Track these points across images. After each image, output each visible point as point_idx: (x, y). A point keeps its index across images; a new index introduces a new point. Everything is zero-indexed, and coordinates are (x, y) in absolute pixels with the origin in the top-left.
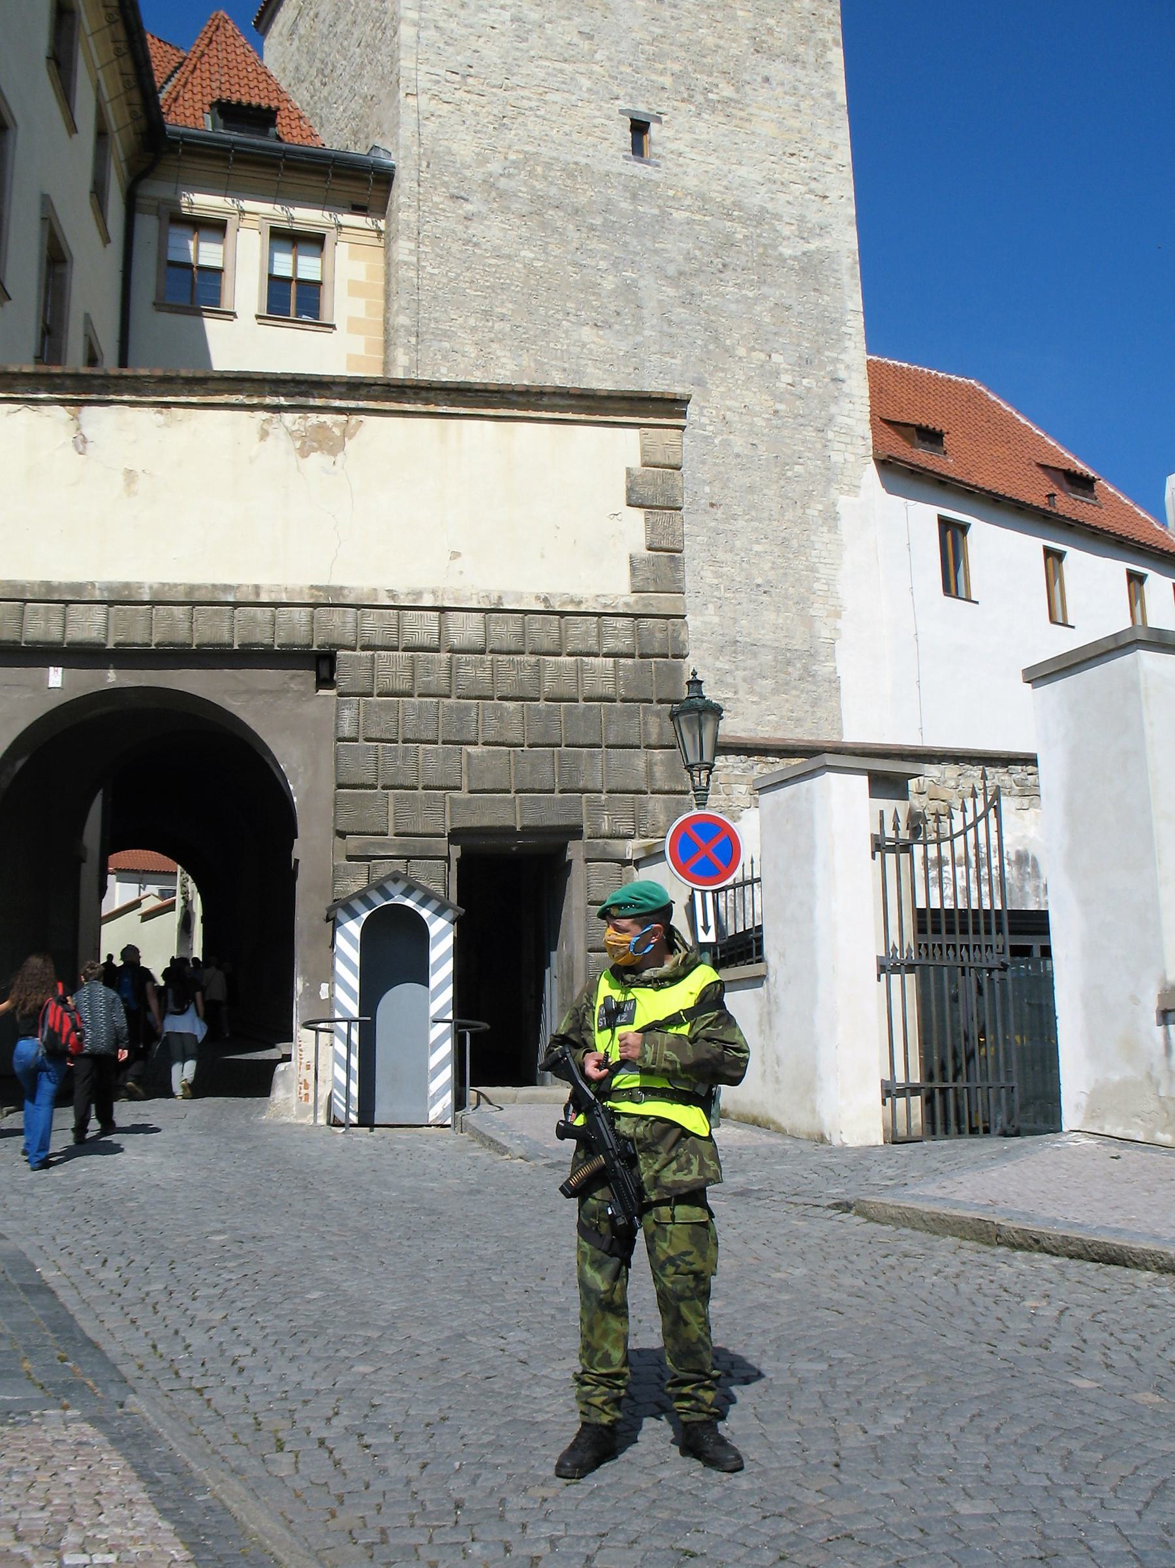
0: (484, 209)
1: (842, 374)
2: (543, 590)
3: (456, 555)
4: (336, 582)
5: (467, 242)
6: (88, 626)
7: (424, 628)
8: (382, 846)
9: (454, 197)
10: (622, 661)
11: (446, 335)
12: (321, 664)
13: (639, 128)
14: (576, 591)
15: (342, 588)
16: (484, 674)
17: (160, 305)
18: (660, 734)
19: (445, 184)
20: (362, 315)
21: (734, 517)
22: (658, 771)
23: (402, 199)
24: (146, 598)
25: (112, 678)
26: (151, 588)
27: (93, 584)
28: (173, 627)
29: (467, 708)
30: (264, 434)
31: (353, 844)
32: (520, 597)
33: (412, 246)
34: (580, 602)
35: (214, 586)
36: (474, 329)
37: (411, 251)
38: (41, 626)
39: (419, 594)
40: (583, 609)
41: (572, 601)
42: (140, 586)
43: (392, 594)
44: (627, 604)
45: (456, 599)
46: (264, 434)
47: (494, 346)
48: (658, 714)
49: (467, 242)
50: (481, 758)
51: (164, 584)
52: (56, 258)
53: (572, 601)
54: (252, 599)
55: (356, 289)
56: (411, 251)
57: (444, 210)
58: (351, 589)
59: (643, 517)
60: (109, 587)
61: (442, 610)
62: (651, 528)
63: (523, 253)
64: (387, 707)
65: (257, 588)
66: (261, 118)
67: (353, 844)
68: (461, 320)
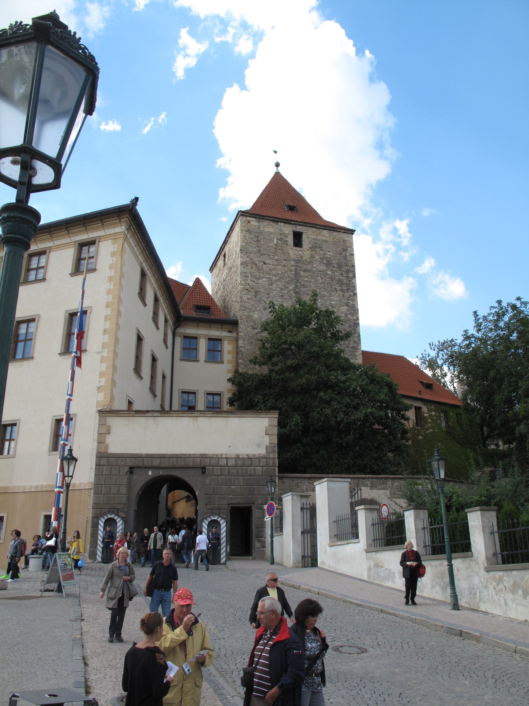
2: (248, 453)
3: (230, 447)
4: (206, 453)
6: (156, 462)
9: (254, 328)
10: (264, 468)
12: (203, 470)
16: (235, 471)
17: (181, 360)
19: (251, 325)
20: (231, 359)
25: (161, 472)
28: (173, 462)
31: (208, 507)
32: (243, 455)
33: (243, 342)
42: (167, 454)
43: (217, 455)
61: (227, 458)
66: (207, 309)
67: (208, 507)
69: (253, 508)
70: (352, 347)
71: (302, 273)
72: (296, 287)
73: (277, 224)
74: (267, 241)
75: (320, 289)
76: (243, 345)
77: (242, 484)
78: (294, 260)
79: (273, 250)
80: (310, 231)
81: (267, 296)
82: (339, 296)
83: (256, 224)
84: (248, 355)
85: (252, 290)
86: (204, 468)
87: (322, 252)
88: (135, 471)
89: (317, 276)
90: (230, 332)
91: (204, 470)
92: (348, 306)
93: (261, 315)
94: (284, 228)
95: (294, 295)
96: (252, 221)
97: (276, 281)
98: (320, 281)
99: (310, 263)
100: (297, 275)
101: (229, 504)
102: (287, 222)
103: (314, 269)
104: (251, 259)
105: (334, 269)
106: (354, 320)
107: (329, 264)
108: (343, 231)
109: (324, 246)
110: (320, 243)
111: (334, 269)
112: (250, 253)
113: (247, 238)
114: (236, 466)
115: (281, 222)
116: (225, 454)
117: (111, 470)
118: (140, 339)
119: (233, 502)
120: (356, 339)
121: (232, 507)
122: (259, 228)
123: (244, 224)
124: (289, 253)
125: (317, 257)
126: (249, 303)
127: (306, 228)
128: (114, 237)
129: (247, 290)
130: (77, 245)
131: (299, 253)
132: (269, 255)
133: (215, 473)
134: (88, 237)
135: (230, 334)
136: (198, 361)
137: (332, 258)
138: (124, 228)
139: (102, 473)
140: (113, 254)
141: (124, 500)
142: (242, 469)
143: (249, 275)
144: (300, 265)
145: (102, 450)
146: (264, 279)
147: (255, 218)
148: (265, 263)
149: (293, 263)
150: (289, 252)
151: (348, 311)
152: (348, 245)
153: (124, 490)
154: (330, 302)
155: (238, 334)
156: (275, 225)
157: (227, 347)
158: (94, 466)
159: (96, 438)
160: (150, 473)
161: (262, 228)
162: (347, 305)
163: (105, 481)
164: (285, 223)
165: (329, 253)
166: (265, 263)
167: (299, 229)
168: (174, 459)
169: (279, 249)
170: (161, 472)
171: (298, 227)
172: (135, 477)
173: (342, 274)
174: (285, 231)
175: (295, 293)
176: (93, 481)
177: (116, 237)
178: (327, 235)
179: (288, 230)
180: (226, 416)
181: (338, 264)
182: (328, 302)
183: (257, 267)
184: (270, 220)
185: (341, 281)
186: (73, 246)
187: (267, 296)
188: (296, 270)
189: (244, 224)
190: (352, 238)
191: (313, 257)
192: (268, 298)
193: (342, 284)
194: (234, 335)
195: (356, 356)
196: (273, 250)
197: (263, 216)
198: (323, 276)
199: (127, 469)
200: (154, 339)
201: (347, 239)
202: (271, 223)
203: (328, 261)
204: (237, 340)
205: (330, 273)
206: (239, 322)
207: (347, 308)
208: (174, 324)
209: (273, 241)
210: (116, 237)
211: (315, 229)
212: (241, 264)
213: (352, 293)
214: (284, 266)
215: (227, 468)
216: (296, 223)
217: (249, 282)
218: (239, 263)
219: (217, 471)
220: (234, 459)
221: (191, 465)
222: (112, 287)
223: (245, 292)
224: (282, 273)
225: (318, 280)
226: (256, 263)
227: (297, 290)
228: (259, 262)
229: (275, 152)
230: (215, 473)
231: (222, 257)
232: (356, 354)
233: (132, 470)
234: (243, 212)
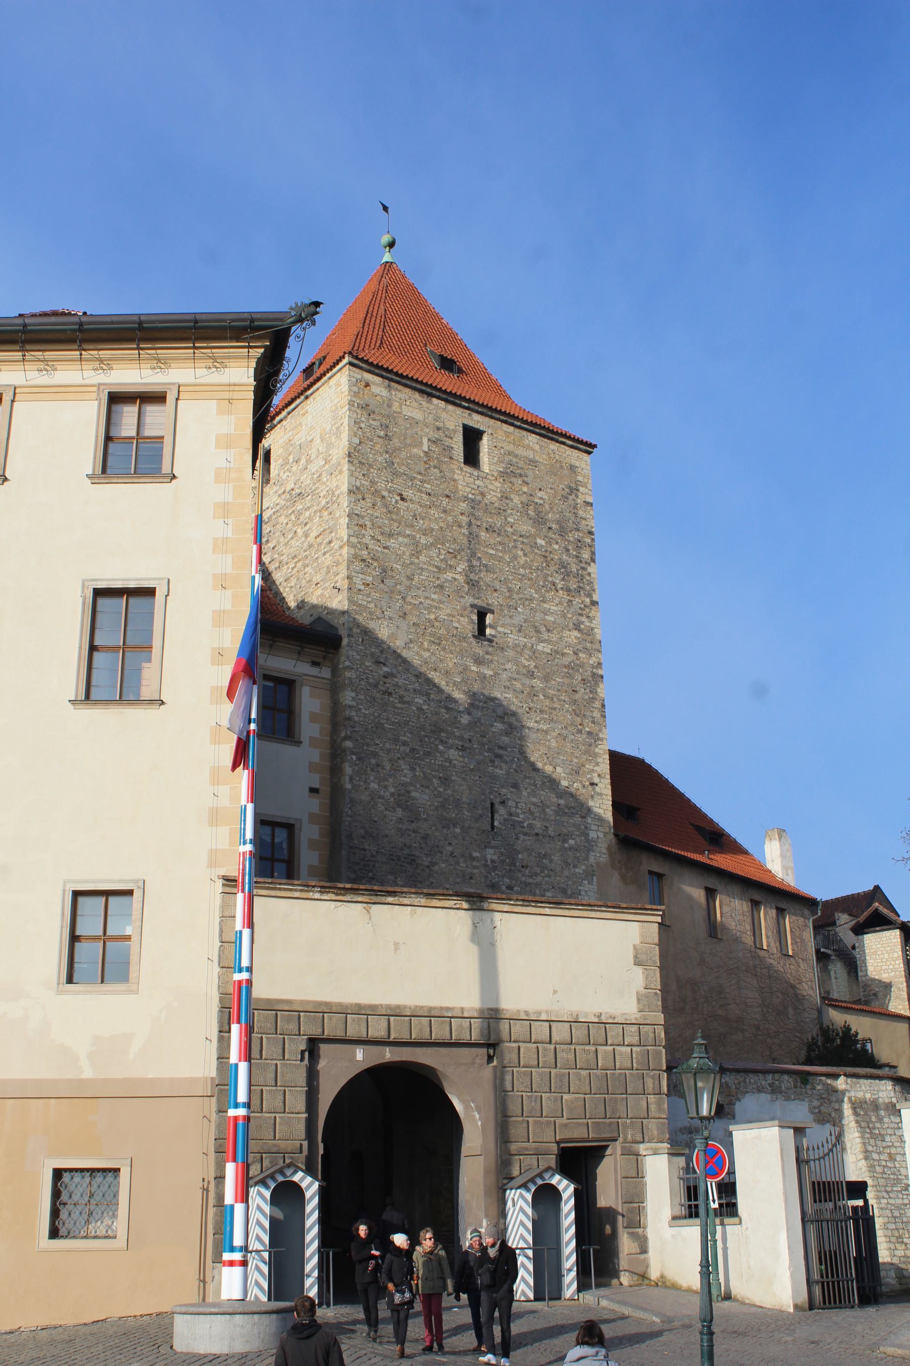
0: (394, 671)
1: (596, 780)
2: (597, 1010)
5: (384, 693)
6: (377, 1029)
8: (526, 1149)
9: (378, 662)
10: (634, 1049)
11: (375, 754)
13: (482, 616)
18: (654, 1088)
19: (372, 655)
20: (317, 735)
21: (536, 875)
22: (653, 1107)
23: (347, 663)
25: (388, 1055)
27: (382, 1005)
33: (353, 695)
36: (389, 751)
37: (353, 698)
38: (354, 1030)
39: (540, 1013)
42: (405, 1007)
43: (527, 1013)
44: (636, 1019)
47: (401, 762)
48: (652, 1077)
49: (384, 693)
51: (417, 1007)
54: (460, 1015)
55: (314, 718)
56: (353, 698)
57: (372, 671)
58: (507, 1010)
60: (388, 1007)
63: (417, 700)
65: (462, 1009)
68: (381, 745)
70: (589, 733)
71: (483, 534)
72: (471, 567)
73: (430, 402)
74: (408, 441)
75: (521, 580)
76: (354, 703)
78: (466, 499)
79: (421, 467)
80: (500, 433)
81: (408, 583)
82: (561, 603)
83: (384, 393)
84: (367, 730)
85: (375, 564)
87: (525, 489)
89: (515, 547)
90: (315, 664)
92: (580, 630)
93: (393, 629)
94: (444, 415)
95: (466, 588)
96: (377, 384)
97: (427, 547)
98: (522, 560)
99: (500, 511)
100: (472, 537)
102: (452, 398)
103: (510, 530)
104: (373, 482)
105: (551, 535)
106: (593, 667)
107: (539, 520)
108: (571, 443)
109: (530, 473)
110: (521, 464)
111: (551, 535)
112: (371, 466)
113: (363, 425)
115: (439, 398)
116: (547, 1012)
119: (568, 1135)
120: (596, 714)
122: (389, 406)
123: (356, 389)
124: (455, 480)
125: (516, 500)
126: (368, 595)
127: (492, 422)
128: (226, 395)
129: (363, 560)
131: (477, 482)
132: (412, 479)
134: (139, 381)
135: (314, 671)
136: (298, 743)
137: (547, 507)
143: (368, 524)
144: (479, 514)
146: (400, 539)
147: (382, 376)
148: (403, 499)
149: (463, 505)
150: (456, 477)
151: (580, 643)
152: (580, 478)
153: (297, 1101)
154: (542, 615)
155: (335, 671)
156: (424, 403)
157: (310, 704)
161: (396, 406)
162: (577, 627)
164: (446, 401)
165: (540, 494)
166: (403, 499)
167: (477, 421)
168: (425, 1021)
169: (435, 467)
171: (476, 417)
173: (568, 550)
174: (446, 423)
175: (468, 583)
176: (214, 1074)
178: (537, 447)
179: (455, 419)
180: (548, 911)
181: (558, 522)
182: (539, 616)
183: (386, 506)
184: (414, 389)
185: (565, 567)
187: (408, 583)
188: (470, 524)
189: (356, 389)
191: (507, 498)
192: (409, 588)
193: (568, 575)
194: (326, 673)
195: (596, 755)
196: (421, 467)
197: (401, 376)
198: (527, 549)
201: (577, 464)
202: (417, 395)
203: (538, 513)
204: (334, 688)
205: (543, 543)
206: (345, 641)
207: (576, 633)
209: (421, 443)
211: (511, 429)
212: (350, 492)
213: (588, 600)
214: (445, 511)
216: (471, 406)
217: (367, 540)
218: (345, 488)
223: (358, 566)
224: (441, 528)
225: (515, 558)
226: (385, 494)
227: (472, 576)
228: (390, 492)
229: (385, 209)
232: (597, 750)
233: (313, 1046)
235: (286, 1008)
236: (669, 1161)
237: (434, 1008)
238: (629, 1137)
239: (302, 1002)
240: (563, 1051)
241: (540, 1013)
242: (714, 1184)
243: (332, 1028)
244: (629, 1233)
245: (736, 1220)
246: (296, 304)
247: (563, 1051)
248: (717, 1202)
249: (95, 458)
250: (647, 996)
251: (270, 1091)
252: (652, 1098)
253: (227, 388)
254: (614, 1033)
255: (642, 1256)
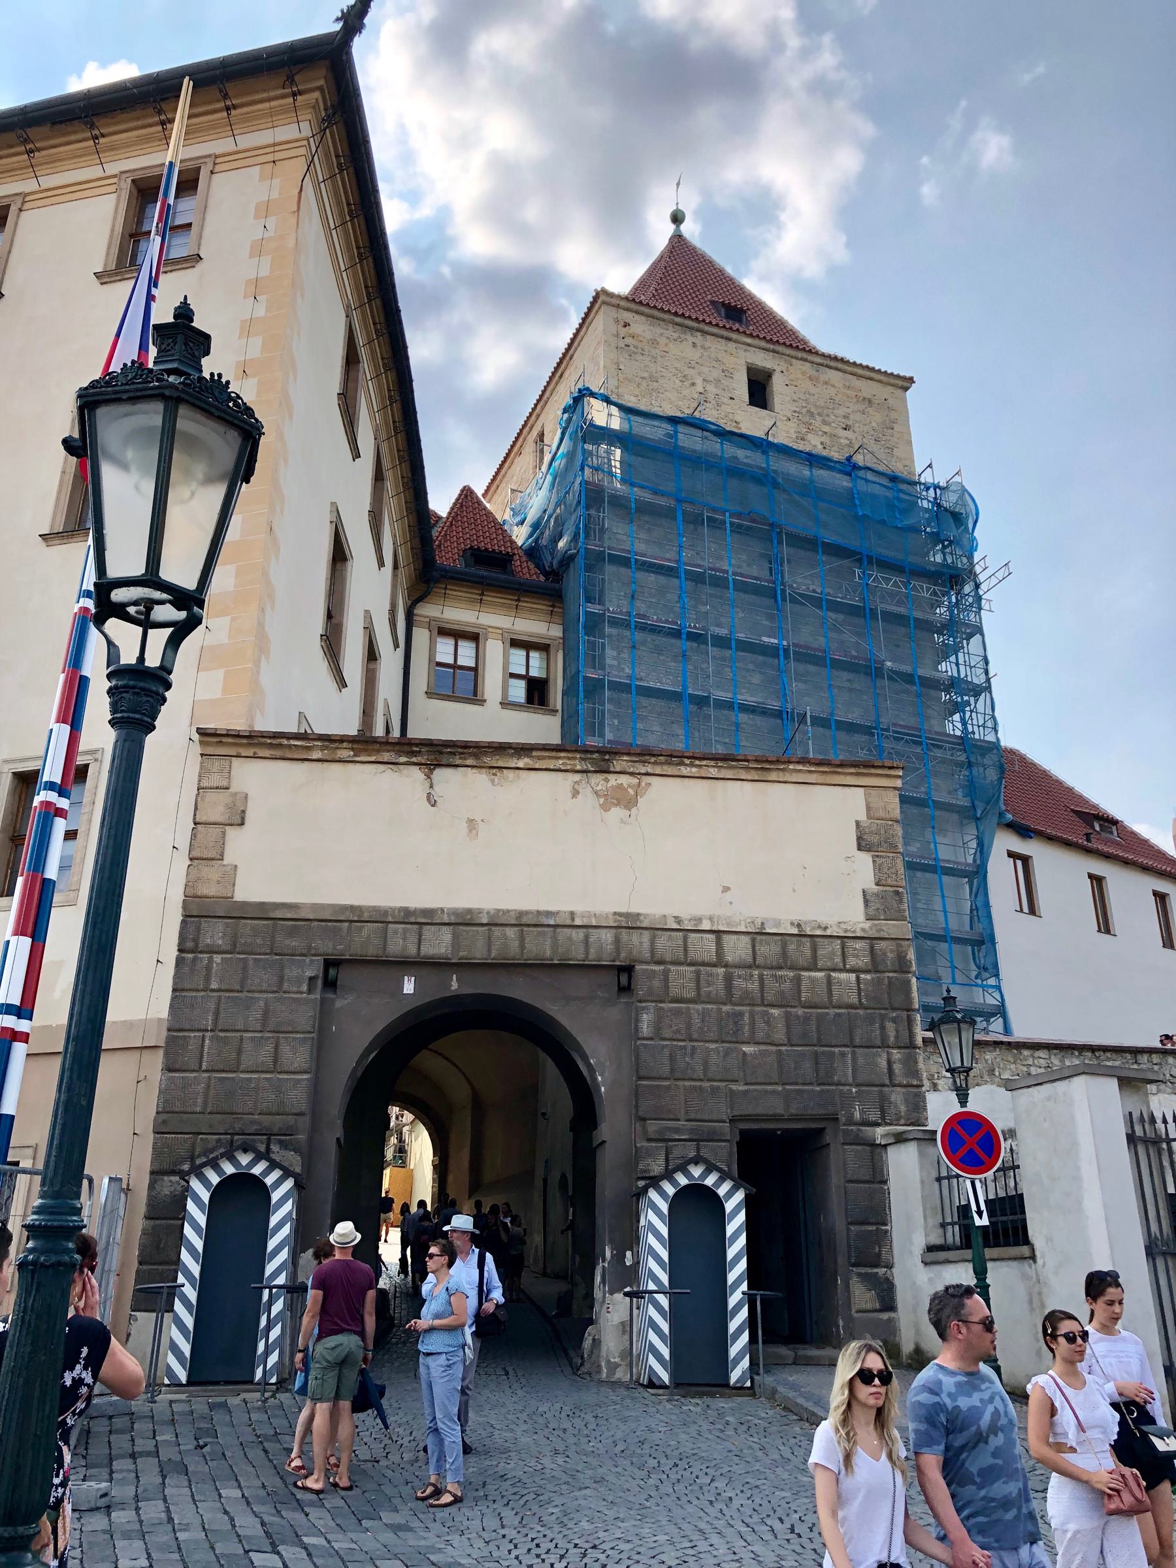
2: (796, 917)
3: (726, 889)
4: (634, 909)
6: (439, 944)
7: (705, 948)
8: (677, 1130)
10: (862, 976)
12: (622, 976)
14: (823, 919)
15: (638, 915)
16: (754, 986)
17: (429, 694)
18: (897, 1037)
22: (897, 1068)
24: (485, 921)
26: (488, 913)
27: (442, 910)
29: (741, 1014)
30: (575, 793)
32: (778, 923)
34: (826, 928)
35: (538, 912)
38: (400, 944)
39: (700, 920)
40: (828, 933)
41: (820, 927)
42: (480, 911)
43: (678, 920)
44: (863, 930)
45: (728, 924)
46: (575, 793)
48: (894, 1020)
50: (754, 1056)
51: (499, 910)
52: (372, 655)
53: (820, 927)
54: (568, 922)
58: (646, 916)
59: (871, 859)
60: (455, 912)
61: (718, 933)
62: (878, 869)
64: (678, 1012)
65: (572, 914)
69: (828, 1138)
76: (615, 663)
77: (780, 1035)
86: (628, 970)
88: (345, 976)
91: (624, 979)
101: (733, 1121)
114: (753, 965)
116: (711, 919)
117: (245, 969)
118: (339, 555)
119: (750, 1110)
121: (743, 1133)
128: (270, 158)
130: (127, 185)
133: (674, 991)
138: (305, 126)
139: (208, 979)
140: (265, 210)
141: (298, 1097)
142: (778, 979)
145: (209, 889)
153: (297, 1056)
158: (170, 953)
159: (184, 843)
160: (409, 987)
163: (217, 1014)
167: (763, 360)
168: (511, 933)
170: (455, 985)
172: (341, 1002)
176: (164, 1013)
177: (278, 156)
186: (112, 188)
190: (905, 401)
199: (313, 969)
200: (373, 588)
208: (411, 590)
210: (278, 156)
215: (721, 971)
219: (681, 980)
220: (746, 940)
221: (577, 955)
222: (261, 311)
230: (674, 991)
231: (530, 447)
233: (332, 973)
234: (611, 295)
235: (289, 916)
236: (921, 1154)
237: (527, 913)
238: (857, 1115)
239: (314, 906)
240: (739, 977)
241: (700, 920)
242: (978, 1185)
243: (364, 942)
244: (859, 1275)
245: (1025, 1250)
246: (342, 11)
247: (739, 977)
248: (985, 1214)
249: (108, 254)
250: (880, 896)
251: (253, 1038)
252: (896, 1054)
253: (271, 149)
254: (829, 952)
255: (885, 1316)
